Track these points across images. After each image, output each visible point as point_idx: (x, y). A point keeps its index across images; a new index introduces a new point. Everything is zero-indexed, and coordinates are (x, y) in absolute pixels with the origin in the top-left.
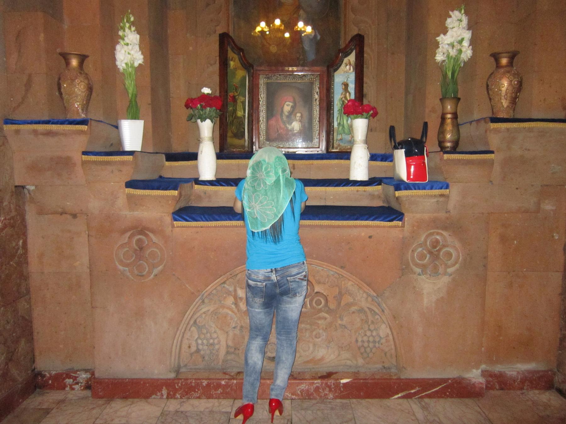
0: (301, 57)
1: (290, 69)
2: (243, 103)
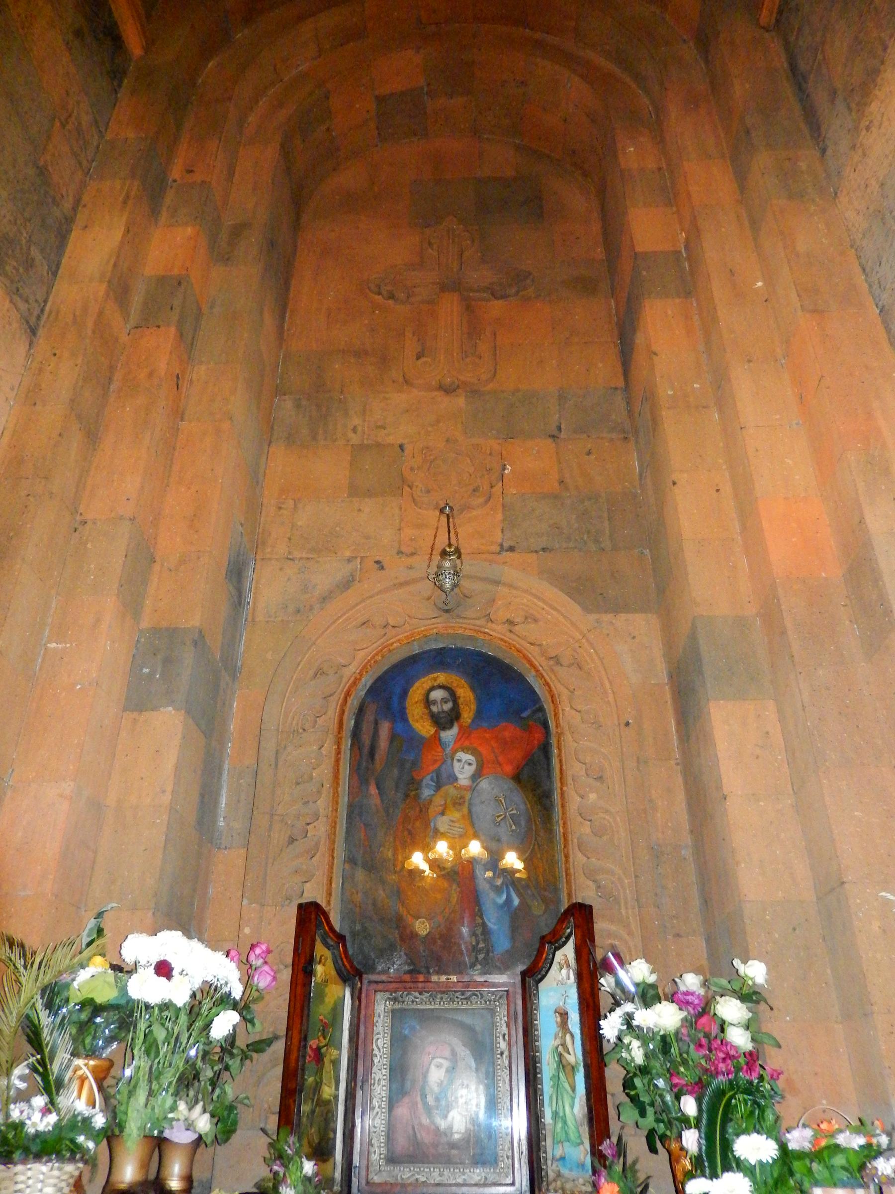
0: (481, 945)
1: (443, 978)
2: (336, 1063)
